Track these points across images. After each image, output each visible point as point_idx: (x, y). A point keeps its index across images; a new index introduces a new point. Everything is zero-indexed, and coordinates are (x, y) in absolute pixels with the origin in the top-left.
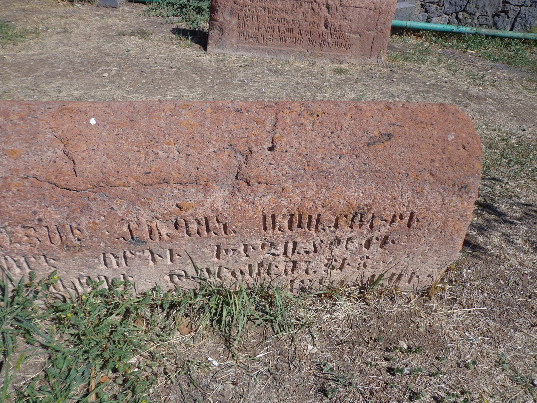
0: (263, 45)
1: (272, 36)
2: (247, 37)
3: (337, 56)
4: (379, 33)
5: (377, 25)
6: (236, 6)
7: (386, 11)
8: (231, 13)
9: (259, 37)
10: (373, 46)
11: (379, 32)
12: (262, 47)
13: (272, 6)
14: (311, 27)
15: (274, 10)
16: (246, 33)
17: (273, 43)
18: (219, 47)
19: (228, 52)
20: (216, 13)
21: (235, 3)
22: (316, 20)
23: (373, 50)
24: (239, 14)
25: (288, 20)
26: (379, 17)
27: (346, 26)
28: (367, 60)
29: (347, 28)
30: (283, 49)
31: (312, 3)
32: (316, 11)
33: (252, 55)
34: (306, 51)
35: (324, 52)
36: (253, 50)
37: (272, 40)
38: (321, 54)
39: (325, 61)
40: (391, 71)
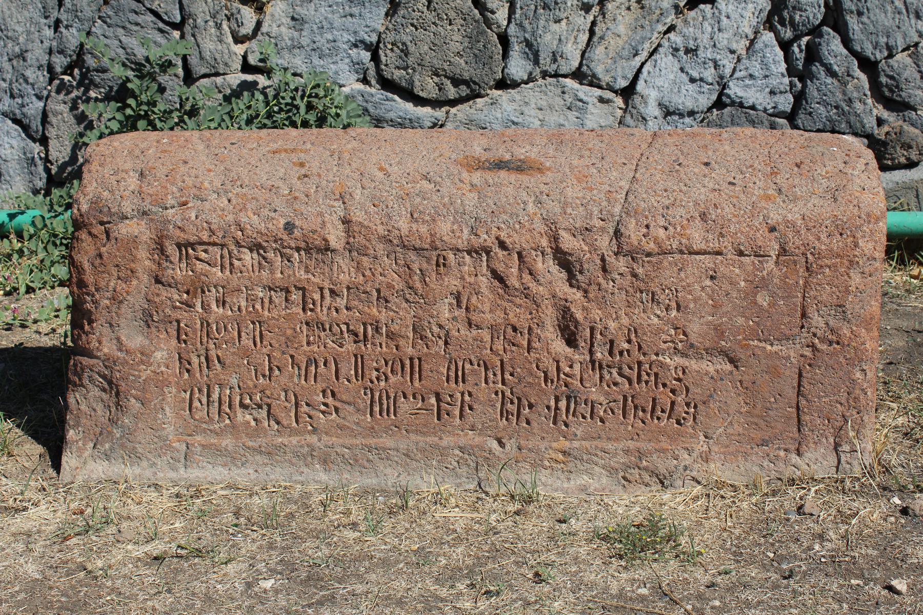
0: (296, 433)
1: (333, 395)
2: (225, 408)
3: (641, 455)
4: (823, 347)
5: (804, 315)
6: (164, 293)
7: (838, 256)
8: (148, 319)
9: (274, 403)
10: (803, 402)
11: (822, 340)
12: (294, 440)
13: (316, 280)
14: (499, 346)
15: (327, 293)
16: (217, 389)
17: (339, 420)
18: (108, 457)
19: (148, 473)
20: (87, 327)
21: (158, 281)
22: (519, 315)
23: (806, 418)
24: (178, 322)
25: (395, 327)
26: (806, 283)
27: (659, 331)
28: (786, 461)
29: (664, 337)
30: (387, 441)
31: (488, 253)
32: (514, 282)
33: (253, 476)
34: (495, 445)
35: (576, 444)
36: (258, 457)
37: (337, 410)
38: (564, 453)
39: (585, 479)
40: (905, 511)
